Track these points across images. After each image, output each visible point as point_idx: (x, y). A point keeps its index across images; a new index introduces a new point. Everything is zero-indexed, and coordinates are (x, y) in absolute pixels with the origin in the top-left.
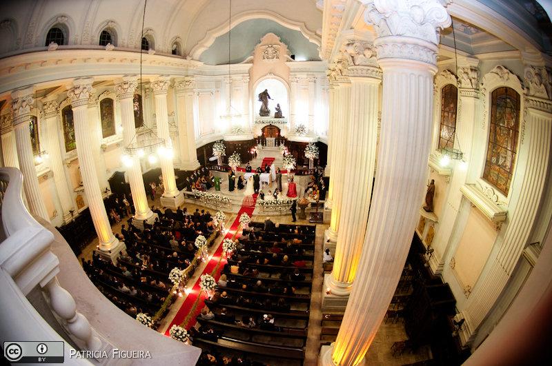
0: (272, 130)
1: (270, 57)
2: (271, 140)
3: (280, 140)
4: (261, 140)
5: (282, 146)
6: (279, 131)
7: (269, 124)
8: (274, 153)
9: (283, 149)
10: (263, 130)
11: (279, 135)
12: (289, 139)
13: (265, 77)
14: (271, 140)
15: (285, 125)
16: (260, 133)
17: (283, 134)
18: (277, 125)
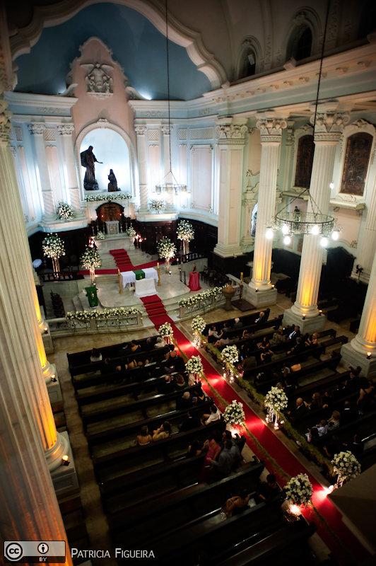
0: (110, 210)
1: (100, 87)
2: (112, 224)
3: (126, 223)
4: (97, 227)
5: (132, 231)
6: (122, 209)
7: (106, 201)
8: (120, 242)
9: (135, 236)
10: (98, 211)
11: (123, 215)
12: (141, 219)
13: (93, 125)
14: (112, 224)
15: (131, 201)
16: (94, 217)
17: (128, 213)
18: (118, 201)
